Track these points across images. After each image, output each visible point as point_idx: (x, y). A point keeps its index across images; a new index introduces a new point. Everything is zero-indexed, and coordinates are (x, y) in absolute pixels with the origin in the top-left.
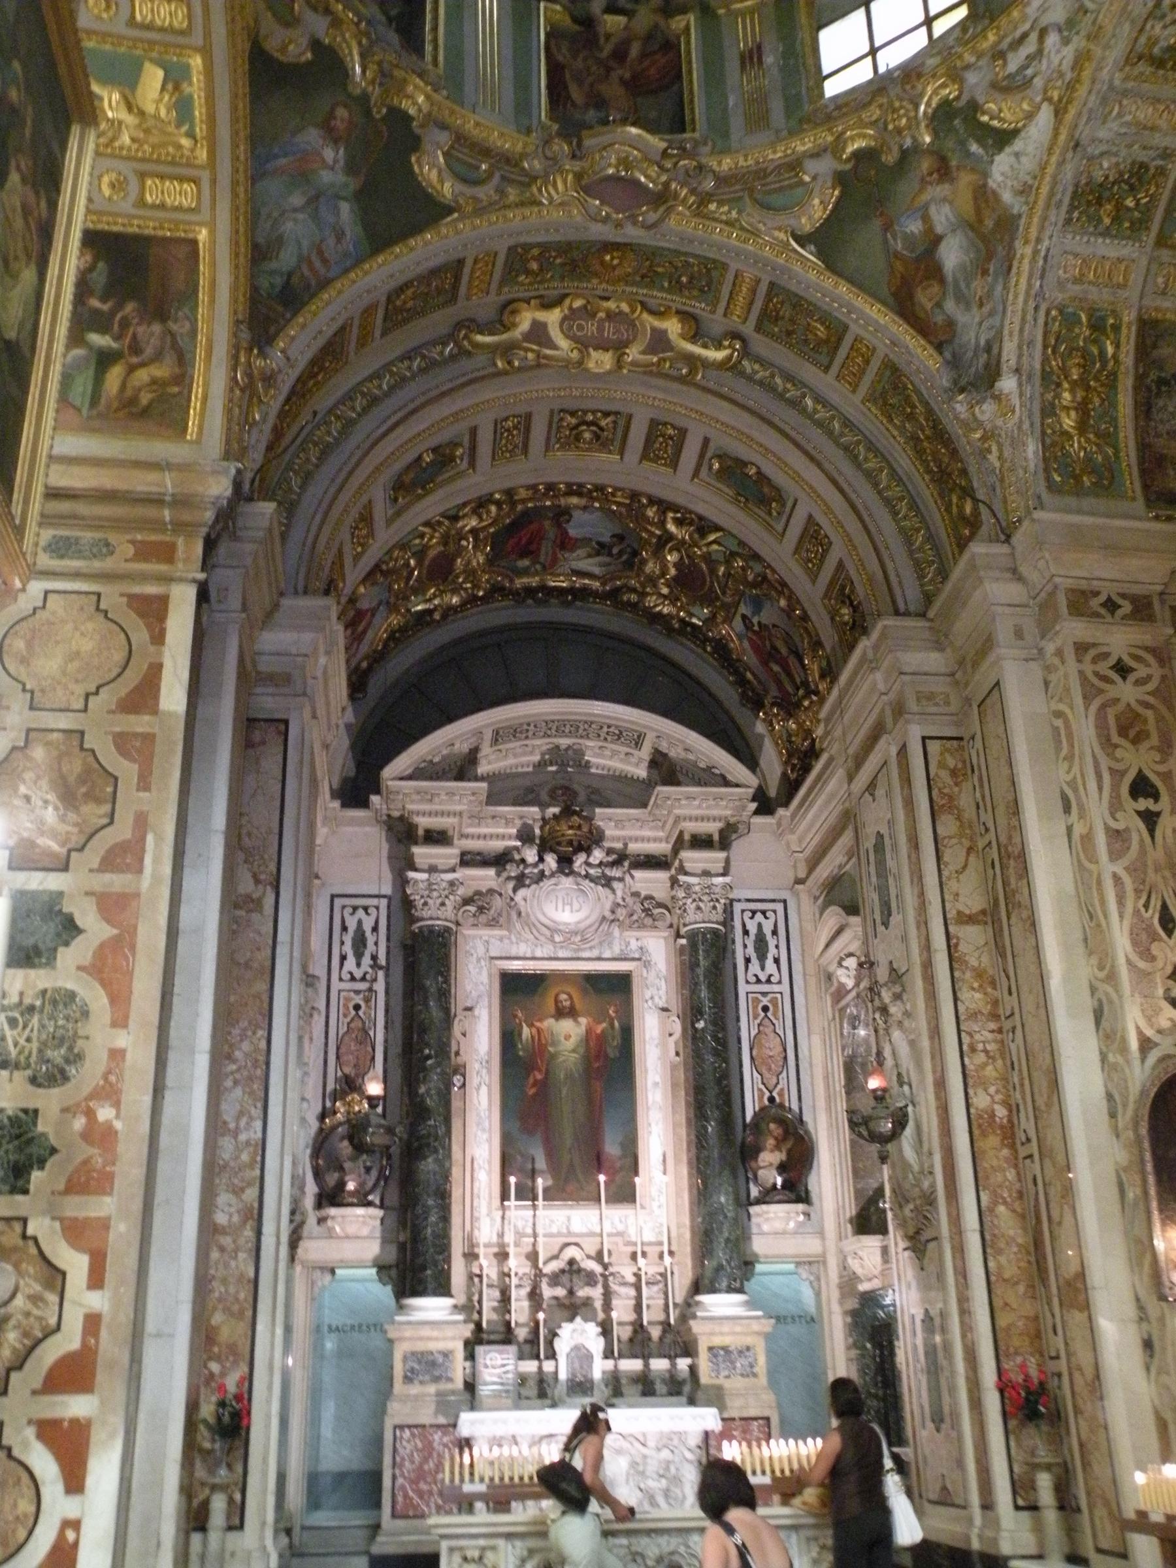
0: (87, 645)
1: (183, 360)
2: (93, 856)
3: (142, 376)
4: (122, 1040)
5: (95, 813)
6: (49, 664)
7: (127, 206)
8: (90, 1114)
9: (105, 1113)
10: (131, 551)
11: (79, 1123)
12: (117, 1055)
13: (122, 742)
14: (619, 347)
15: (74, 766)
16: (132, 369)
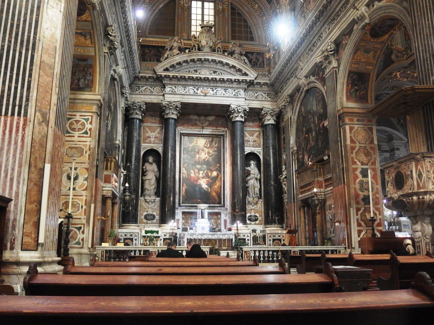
0: (364, 135)
1: (367, 91)
2: (370, 163)
3: (362, 93)
4: (378, 187)
5: (370, 158)
6: (360, 137)
7: (363, 69)
8: (376, 196)
9: (377, 195)
10: (367, 121)
11: (375, 197)
12: (377, 188)
13: (371, 148)
14: (408, 78)
15: (366, 151)
16: (360, 92)
